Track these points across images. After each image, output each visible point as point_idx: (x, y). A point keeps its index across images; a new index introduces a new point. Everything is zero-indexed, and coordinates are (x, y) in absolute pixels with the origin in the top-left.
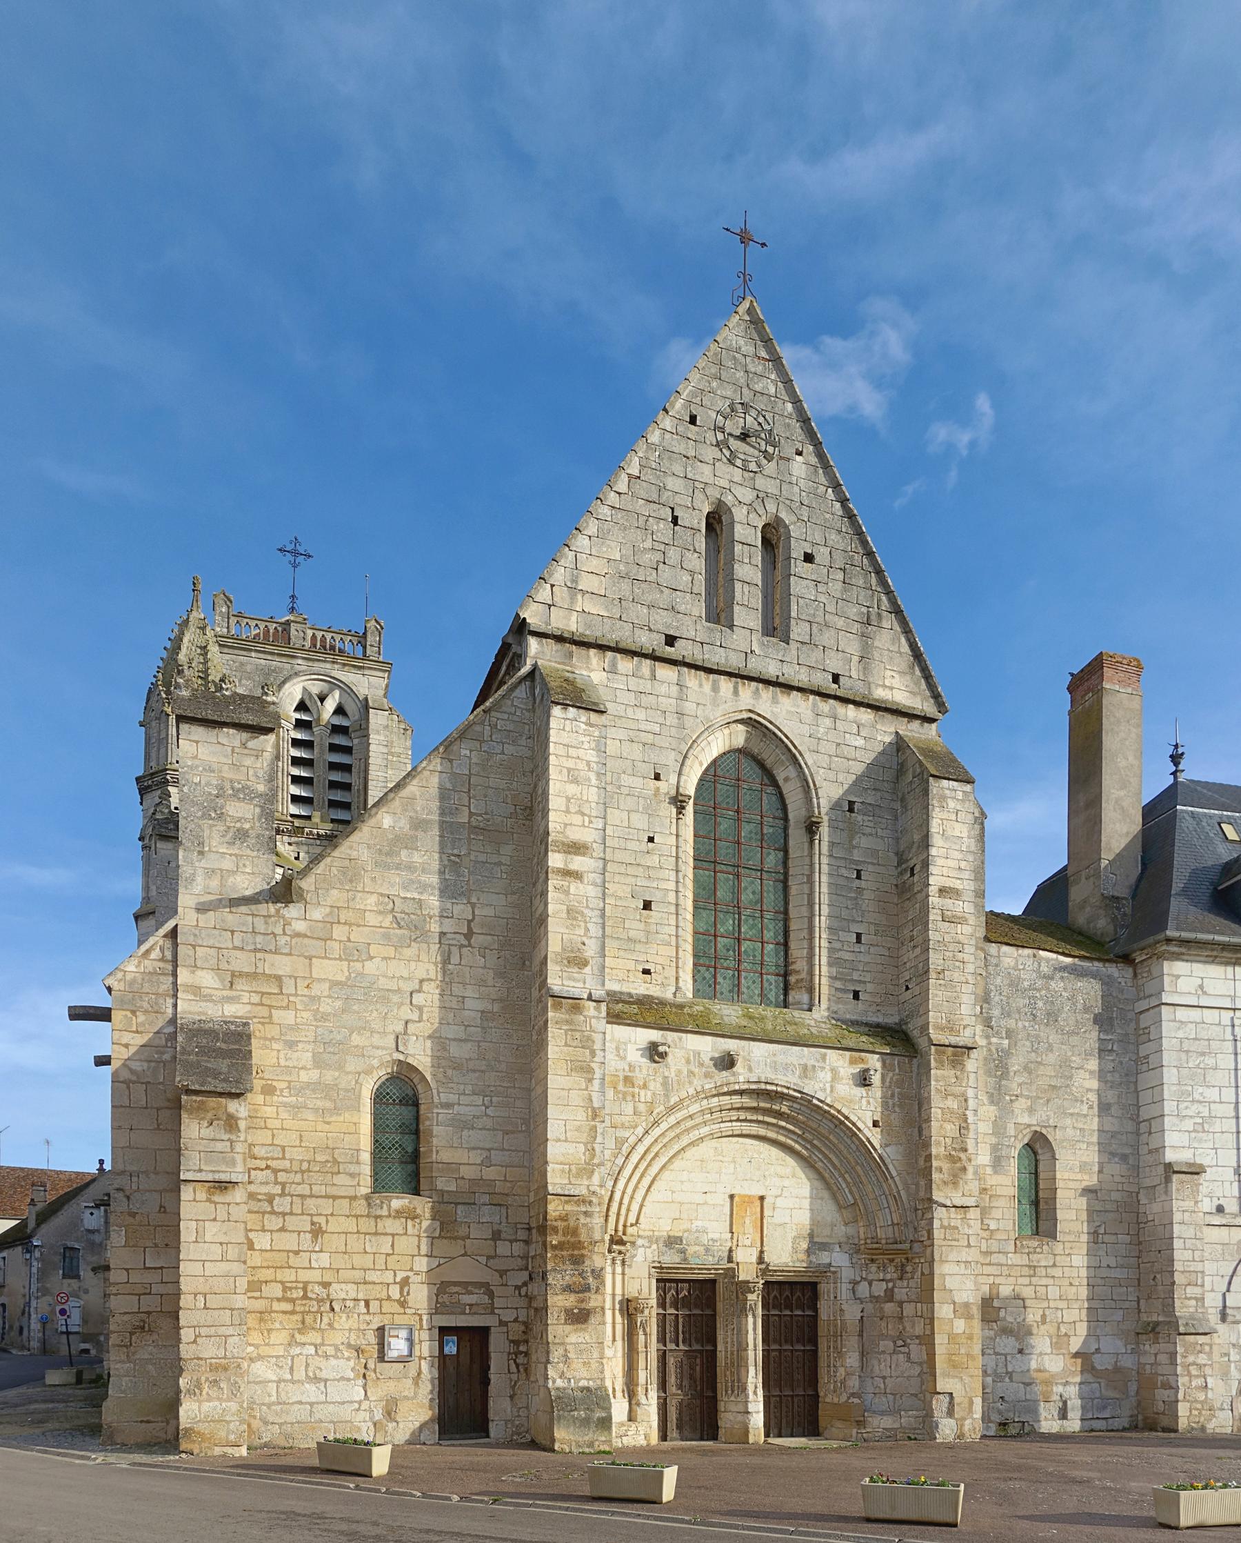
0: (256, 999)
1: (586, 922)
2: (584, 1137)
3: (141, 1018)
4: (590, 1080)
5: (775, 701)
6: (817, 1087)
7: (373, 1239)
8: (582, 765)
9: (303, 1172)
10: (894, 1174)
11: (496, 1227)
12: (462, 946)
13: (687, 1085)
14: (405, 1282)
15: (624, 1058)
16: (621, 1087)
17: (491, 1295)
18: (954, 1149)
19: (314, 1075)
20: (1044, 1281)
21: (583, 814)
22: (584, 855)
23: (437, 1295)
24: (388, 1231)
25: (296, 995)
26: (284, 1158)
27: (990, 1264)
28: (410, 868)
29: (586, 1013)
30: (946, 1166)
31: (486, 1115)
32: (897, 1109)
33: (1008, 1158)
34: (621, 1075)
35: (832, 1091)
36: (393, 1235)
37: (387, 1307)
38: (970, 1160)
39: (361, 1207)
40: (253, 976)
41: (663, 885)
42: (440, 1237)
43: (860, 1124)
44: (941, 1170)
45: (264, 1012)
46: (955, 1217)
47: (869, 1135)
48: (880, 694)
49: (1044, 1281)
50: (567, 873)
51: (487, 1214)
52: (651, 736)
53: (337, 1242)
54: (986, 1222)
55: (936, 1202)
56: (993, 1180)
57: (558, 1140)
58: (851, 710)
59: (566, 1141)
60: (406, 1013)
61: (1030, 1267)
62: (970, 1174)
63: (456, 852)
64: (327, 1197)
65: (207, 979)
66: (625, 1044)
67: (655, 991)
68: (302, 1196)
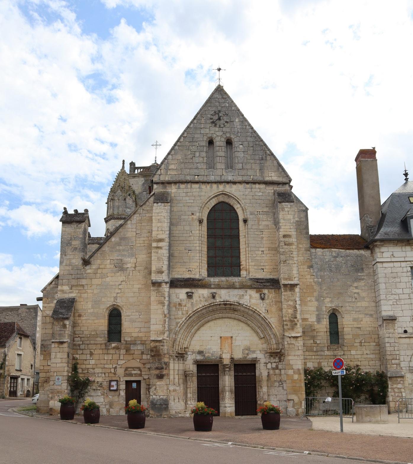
0: (77, 291)
1: (163, 260)
2: (162, 323)
3: (49, 300)
4: (164, 306)
6: (244, 301)
7: (107, 355)
8: (162, 217)
9: (88, 337)
10: (274, 327)
11: (142, 351)
12: (133, 270)
13: (199, 304)
14: (116, 368)
15: (179, 298)
16: (177, 307)
18: (292, 318)
19: (92, 310)
21: (163, 231)
22: (163, 242)
23: (125, 371)
24: (111, 353)
25: (88, 289)
26: (83, 334)
27: (317, 355)
28: (119, 251)
29: (162, 287)
30: (289, 323)
31: (140, 318)
32: (274, 306)
34: (178, 303)
35: (250, 302)
36: (112, 354)
37: (111, 375)
38: (298, 321)
39: (103, 347)
41: (195, 245)
42: (126, 354)
43: (260, 312)
44: (287, 325)
45: (79, 295)
46: (293, 341)
47: (264, 315)
48: (267, 179)
50: (158, 248)
51: (140, 347)
52: (191, 204)
53: (96, 357)
54: (315, 341)
55: (286, 336)
56: (317, 326)
57: (154, 324)
58: (257, 186)
59: (156, 324)
60: (117, 291)
61: (334, 355)
62: (298, 325)
63: (132, 245)
64: (94, 344)
65: (66, 288)
66: (179, 294)
67: (192, 276)
68: (88, 344)
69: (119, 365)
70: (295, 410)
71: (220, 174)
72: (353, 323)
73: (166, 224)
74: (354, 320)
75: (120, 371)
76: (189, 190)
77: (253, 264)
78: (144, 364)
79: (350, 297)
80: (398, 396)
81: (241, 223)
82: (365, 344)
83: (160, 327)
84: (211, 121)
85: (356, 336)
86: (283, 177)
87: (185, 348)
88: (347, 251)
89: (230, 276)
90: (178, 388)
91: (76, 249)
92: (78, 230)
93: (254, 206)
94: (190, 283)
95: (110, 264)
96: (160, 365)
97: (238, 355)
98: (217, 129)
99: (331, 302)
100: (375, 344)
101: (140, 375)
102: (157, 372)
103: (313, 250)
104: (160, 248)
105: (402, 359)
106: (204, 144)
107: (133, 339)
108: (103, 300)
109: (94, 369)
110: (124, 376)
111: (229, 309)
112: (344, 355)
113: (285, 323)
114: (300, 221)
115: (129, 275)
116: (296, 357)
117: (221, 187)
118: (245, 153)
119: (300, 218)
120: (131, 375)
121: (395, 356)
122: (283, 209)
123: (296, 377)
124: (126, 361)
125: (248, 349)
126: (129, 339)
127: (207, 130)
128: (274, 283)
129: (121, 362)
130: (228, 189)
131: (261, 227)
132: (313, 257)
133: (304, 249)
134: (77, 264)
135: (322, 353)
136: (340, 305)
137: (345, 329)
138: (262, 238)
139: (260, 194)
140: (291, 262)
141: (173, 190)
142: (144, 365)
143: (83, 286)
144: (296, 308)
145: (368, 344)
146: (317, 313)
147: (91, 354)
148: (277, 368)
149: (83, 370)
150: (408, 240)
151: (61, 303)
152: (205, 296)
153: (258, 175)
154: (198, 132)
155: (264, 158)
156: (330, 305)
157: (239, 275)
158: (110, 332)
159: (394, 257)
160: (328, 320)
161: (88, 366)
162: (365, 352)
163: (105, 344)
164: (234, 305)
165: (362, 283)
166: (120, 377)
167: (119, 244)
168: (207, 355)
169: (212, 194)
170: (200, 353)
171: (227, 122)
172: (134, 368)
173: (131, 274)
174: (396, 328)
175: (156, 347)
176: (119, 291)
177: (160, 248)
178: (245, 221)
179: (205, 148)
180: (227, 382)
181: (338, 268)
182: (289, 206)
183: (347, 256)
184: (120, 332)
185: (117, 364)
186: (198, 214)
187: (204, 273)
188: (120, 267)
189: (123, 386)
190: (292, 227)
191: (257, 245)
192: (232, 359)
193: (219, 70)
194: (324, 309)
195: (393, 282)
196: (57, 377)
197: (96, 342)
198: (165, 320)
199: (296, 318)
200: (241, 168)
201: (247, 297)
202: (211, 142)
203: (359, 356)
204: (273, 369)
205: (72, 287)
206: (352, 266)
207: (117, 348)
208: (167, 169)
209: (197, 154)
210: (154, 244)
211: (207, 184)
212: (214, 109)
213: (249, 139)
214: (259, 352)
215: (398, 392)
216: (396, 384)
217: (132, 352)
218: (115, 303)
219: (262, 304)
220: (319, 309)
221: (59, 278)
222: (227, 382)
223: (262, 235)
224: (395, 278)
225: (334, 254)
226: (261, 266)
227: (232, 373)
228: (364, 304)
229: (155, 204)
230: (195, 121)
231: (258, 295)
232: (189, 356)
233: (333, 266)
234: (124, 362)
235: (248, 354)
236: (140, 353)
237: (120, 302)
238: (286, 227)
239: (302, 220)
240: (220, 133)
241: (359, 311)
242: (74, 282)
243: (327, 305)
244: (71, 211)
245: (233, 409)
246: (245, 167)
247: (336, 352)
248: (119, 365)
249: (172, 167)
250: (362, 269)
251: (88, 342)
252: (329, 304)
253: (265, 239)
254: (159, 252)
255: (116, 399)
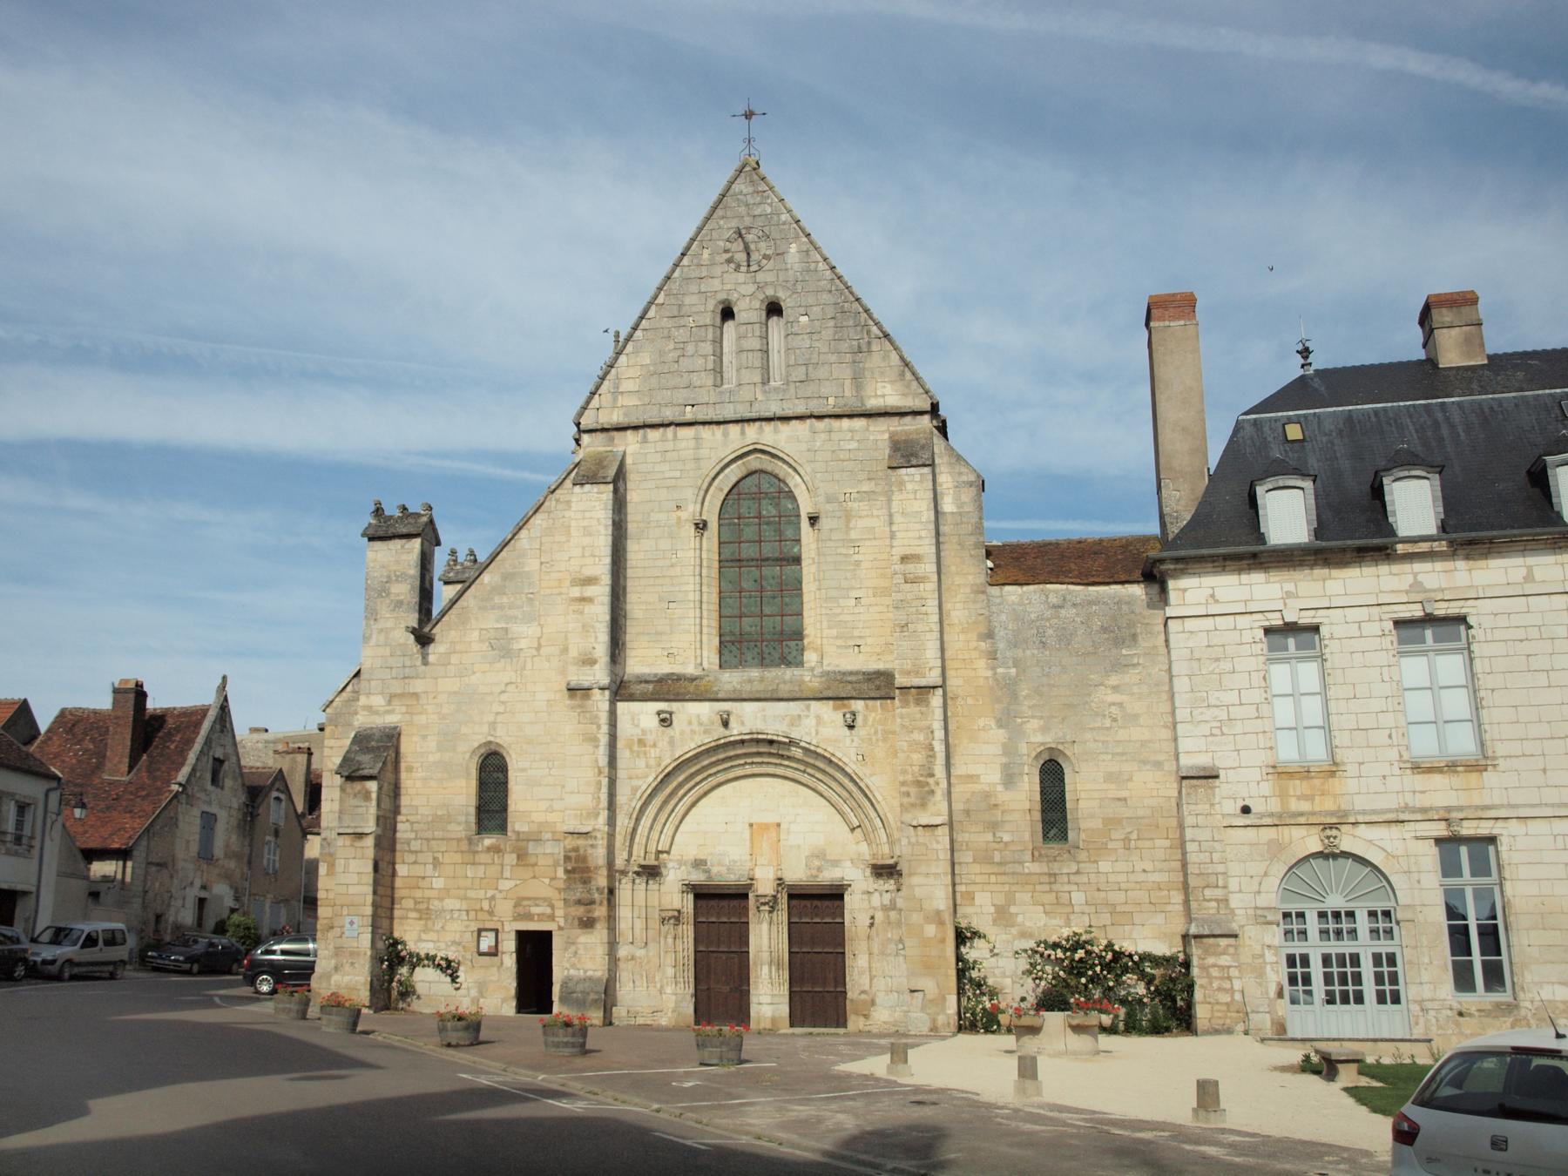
2: (592, 789)
5: (776, 431)
10: (880, 798)
14: (493, 898)
20: (1067, 888)
28: (501, 607)
30: (913, 790)
33: (1021, 774)
37: (481, 916)
39: (464, 846)
40: (402, 695)
44: (908, 794)
48: (873, 403)
49: (1067, 888)
50: (583, 599)
56: (1002, 796)
58: (846, 422)
60: (497, 708)
67: (677, 669)
70: (925, 1017)
71: (749, 397)
72: (1104, 786)
73: (602, 538)
74: (1110, 777)
75: (505, 909)
76: (670, 446)
77: (834, 632)
79: (1097, 715)
80: (1220, 989)
81: (805, 523)
82: (1140, 844)
83: (586, 800)
84: (728, 256)
85: (1111, 822)
86: (915, 395)
87: (659, 852)
88: (1091, 588)
89: (778, 665)
90: (640, 953)
91: (399, 604)
92: (404, 557)
93: (837, 476)
94: (669, 689)
95: (481, 641)
96: (585, 896)
97: (797, 874)
98: (741, 277)
99: (1045, 730)
100: (1167, 843)
101: (552, 918)
102: (580, 911)
103: (995, 591)
104: (589, 600)
105: (1233, 884)
106: (708, 321)
107: (534, 828)
108: (464, 730)
109: (441, 899)
111: (768, 751)
112: (1078, 873)
113: (904, 789)
114: (960, 514)
115: (524, 668)
116: (931, 880)
117: (752, 432)
118: (815, 337)
119: (960, 505)
120: (529, 917)
121: (1212, 879)
122: (901, 484)
123: (931, 930)
125: (820, 855)
126: (525, 829)
127: (716, 282)
128: (880, 686)
129: (506, 885)
130: (769, 436)
131: (853, 535)
132: (994, 609)
133: (968, 590)
134: (402, 641)
135: (1018, 868)
136: (1069, 738)
137: (1082, 804)
138: (858, 563)
139: (854, 445)
140: (920, 627)
141: (630, 444)
143: (415, 695)
144: (932, 749)
145: (1148, 844)
146: (1004, 760)
147: (436, 863)
148: (893, 906)
149: (416, 903)
150: (1254, 555)
151: (362, 740)
152: (705, 719)
153: (848, 393)
154: (693, 288)
155: (864, 348)
156: (1039, 738)
157: (800, 664)
158: (482, 809)
159: (1217, 601)
160: (1037, 780)
161: (428, 893)
162: (1139, 866)
163: (469, 840)
164: (779, 742)
165: (1131, 677)
167: (499, 590)
168: (715, 870)
169: (727, 453)
170: (699, 864)
171: (766, 257)
173: (529, 666)
174: (1217, 800)
175: (576, 849)
176: (501, 709)
177: (589, 600)
178: (813, 520)
179: (711, 330)
180: (767, 939)
181: (1065, 637)
182: (917, 478)
183: (1091, 603)
184: (505, 809)
186: (691, 508)
187: (711, 658)
188: (503, 647)
189: (509, 945)
190: (923, 533)
191: (845, 584)
192: (780, 881)
193: (749, 115)
194: (1023, 748)
195: (1212, 673)
196: (348, 920)
197: (449, 835)
198: (599, 783)
199: (932, 775)
200: (803, 378)
201: (810, 722)
202: (727, 313)
203: (1122, 878)
204: (885, 909)
205: (391, 698)
206: (1104, 629)
207: (496, 849)
208: (616, 393)
209: (690, 348)
210: (576, 592)
211: (714, 427)
212: (734, 224)
213: (825, 297)
214: (848, 863)
215: (1222, 978)
216: (1214, 954)
217: (532, 860)
218: (490, 738)
219: (848, 741)
220: (1009, 750)
221: (363, 676)
222: (767, 939)
223: (856, 557)
224: (1217, 660)
225: (1053, 599)
226: (852, 637)
227: (782, 916)
228: (1137, 733)
229: (577, 489)
230: (685, 261)
231: (838, 716)
232: (672, 872)
233: (1050, 632)
234: (512, 883)
235: (819, 869)
236: (550, 862)
237: (504, 738)
238: (910, 534)
239: (967, 509)
240: (751, 288)
241: (1123, 754)
242: (396, 688)
243: (1032, 739)
244: (391, 510)
245: (784, 1010)
246: (812, 375)
247: (1055, 868)
249: (627, 386)
250: (1134, 637)
251: (428, 835)
252: (1036, 737)
253: (864, 565)
254: (587, 610)
255: (493, 974)
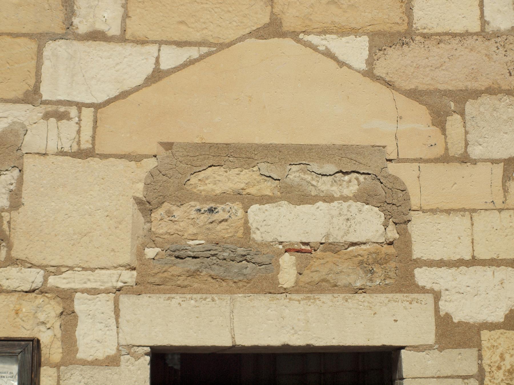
17: (396, 207)
69: (58, 112)
78: (442, 105)
101: (393, 268)
110: (139, 288)
120: (242, 266)
124: (171, 58)
142: (439, 120)
166: (66, 297)
172: (287, 166)
185: (32, 96)
248: (58, 112)
